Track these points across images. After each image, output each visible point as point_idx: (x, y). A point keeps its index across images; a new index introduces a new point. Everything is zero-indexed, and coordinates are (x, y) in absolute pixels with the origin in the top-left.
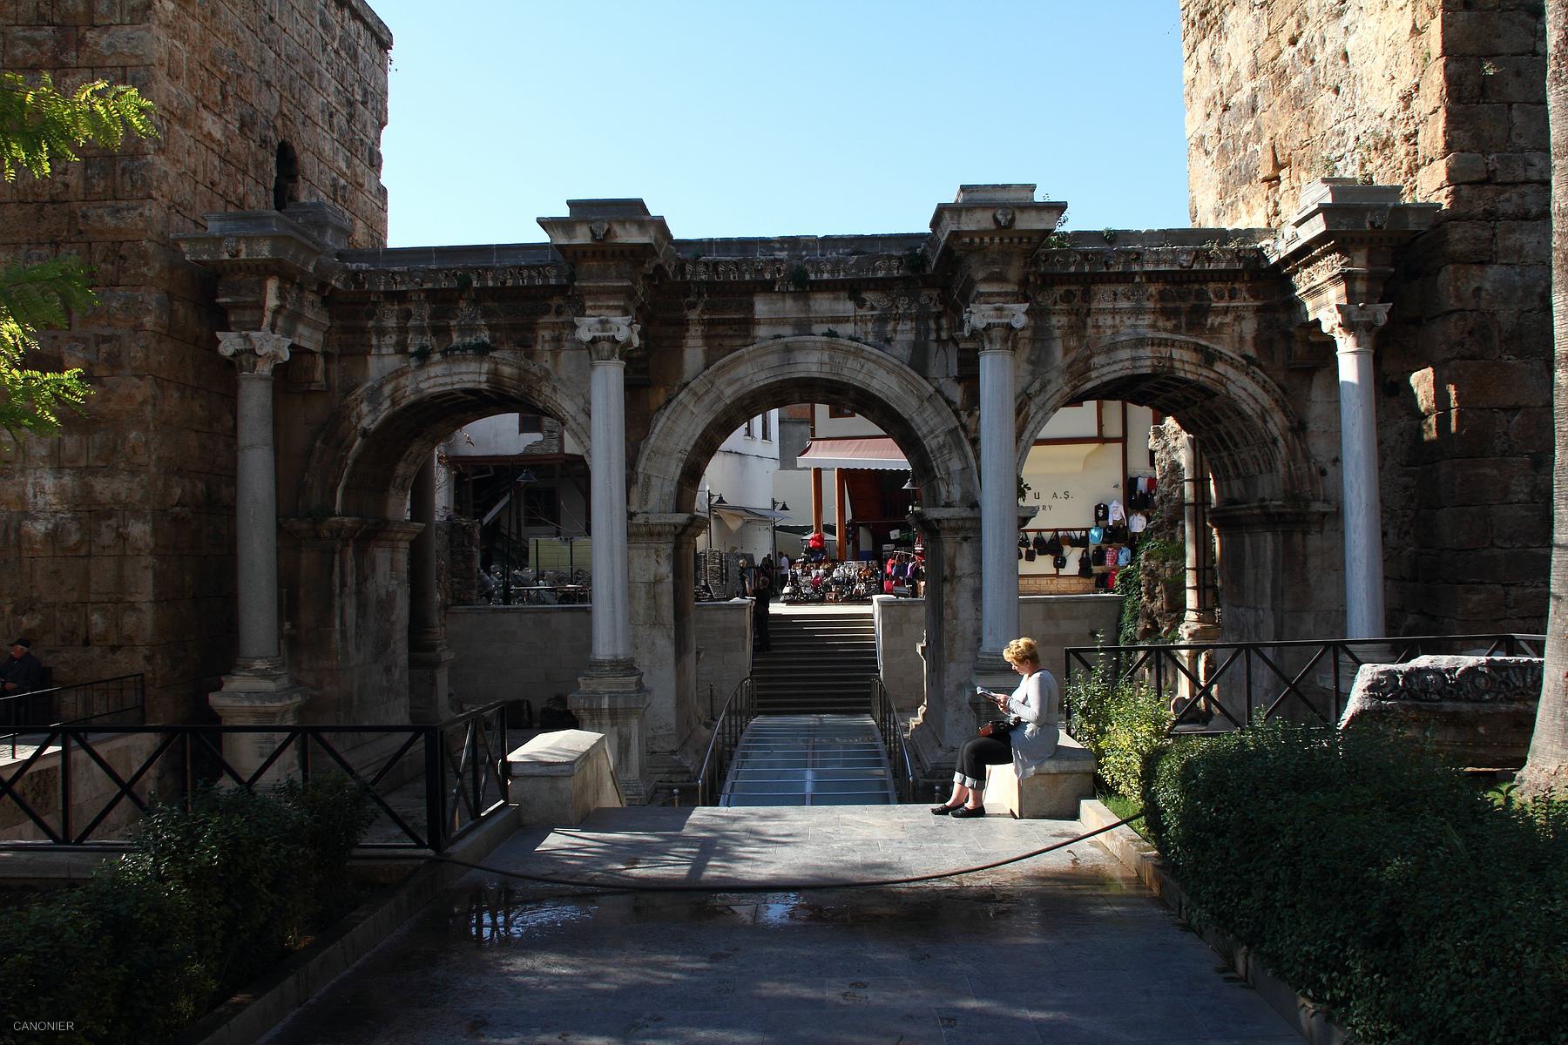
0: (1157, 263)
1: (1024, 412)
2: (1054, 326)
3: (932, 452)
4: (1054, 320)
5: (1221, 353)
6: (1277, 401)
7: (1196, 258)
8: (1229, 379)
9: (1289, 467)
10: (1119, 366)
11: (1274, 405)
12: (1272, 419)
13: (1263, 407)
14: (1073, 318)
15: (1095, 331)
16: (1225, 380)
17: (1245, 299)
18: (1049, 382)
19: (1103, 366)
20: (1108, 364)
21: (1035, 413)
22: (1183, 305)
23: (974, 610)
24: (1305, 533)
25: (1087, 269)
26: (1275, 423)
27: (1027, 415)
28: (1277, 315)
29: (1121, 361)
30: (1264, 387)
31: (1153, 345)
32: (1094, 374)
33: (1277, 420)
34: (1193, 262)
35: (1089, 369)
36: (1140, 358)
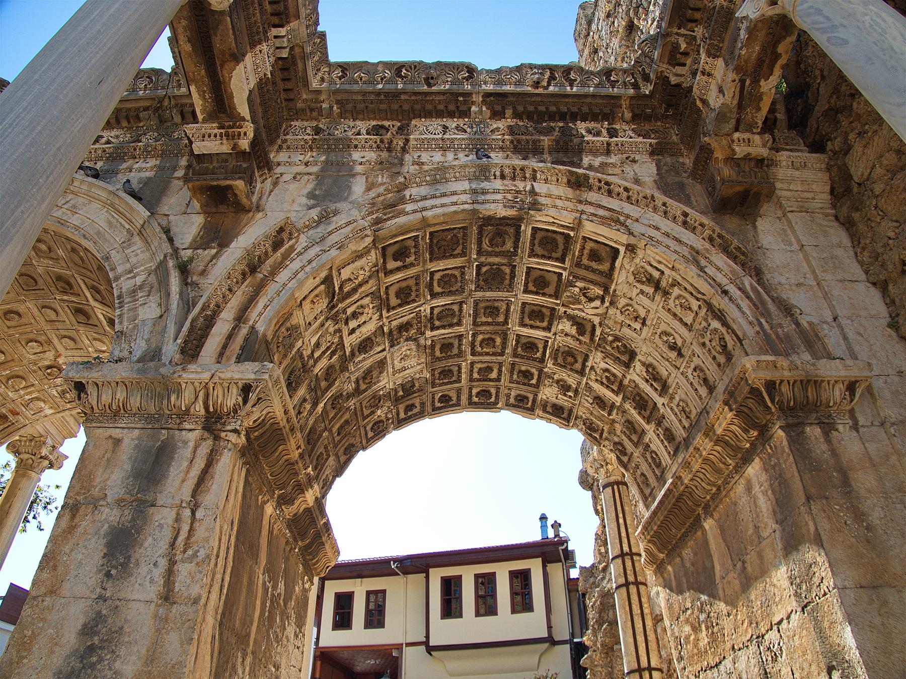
0: (500, 83)
1: (287, 246)
2: (354, 161)
3: (120, 297)
4: (356, 155)
5: (607, 183)
6: (711, 239)
7: (552, 78)
8: (628, 216)
9: (760, 324)
10: (454, 199)
11: (707, 245)
12: (711, 262)
13: (692, 248)
14: (385, 154)
15: (417, 167)
16: (622, 218)
17: (631, 138)
18: (336, 213)
19: (425, 198)
20: (434, 197)
21: (306, 249)
22: (546, 141)
23: (101, 576)
24: (828, 427)
25: (400, 86)
26: (718, 269)
27: (292, 249)
28: (681, 160)
29: (454, 193)
30: (685, 223)
31: (503, 177)
32: (409, 207)
33: (719, 263)
34: (549, 84)
35: (402, 200)
36: (484, 192)
